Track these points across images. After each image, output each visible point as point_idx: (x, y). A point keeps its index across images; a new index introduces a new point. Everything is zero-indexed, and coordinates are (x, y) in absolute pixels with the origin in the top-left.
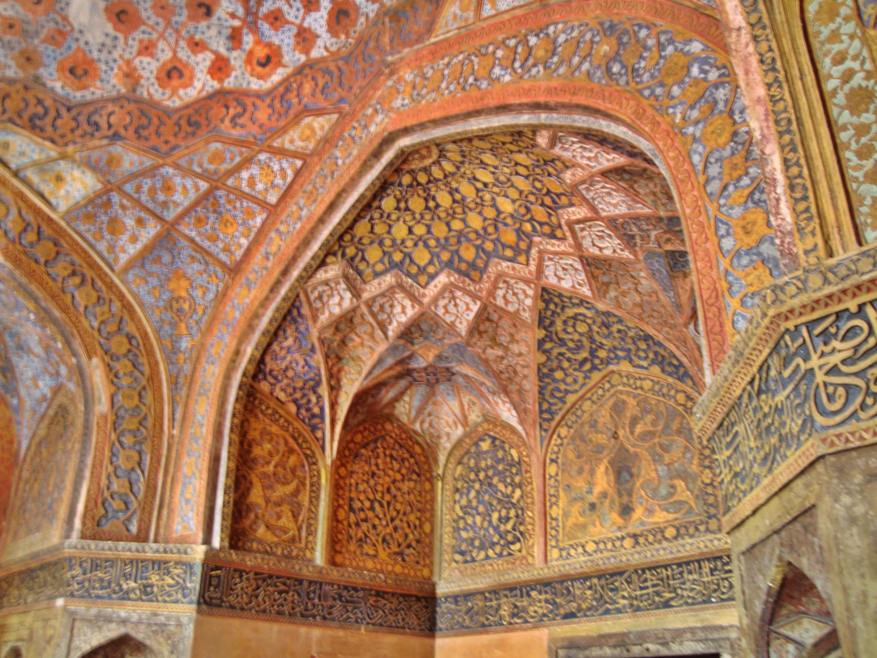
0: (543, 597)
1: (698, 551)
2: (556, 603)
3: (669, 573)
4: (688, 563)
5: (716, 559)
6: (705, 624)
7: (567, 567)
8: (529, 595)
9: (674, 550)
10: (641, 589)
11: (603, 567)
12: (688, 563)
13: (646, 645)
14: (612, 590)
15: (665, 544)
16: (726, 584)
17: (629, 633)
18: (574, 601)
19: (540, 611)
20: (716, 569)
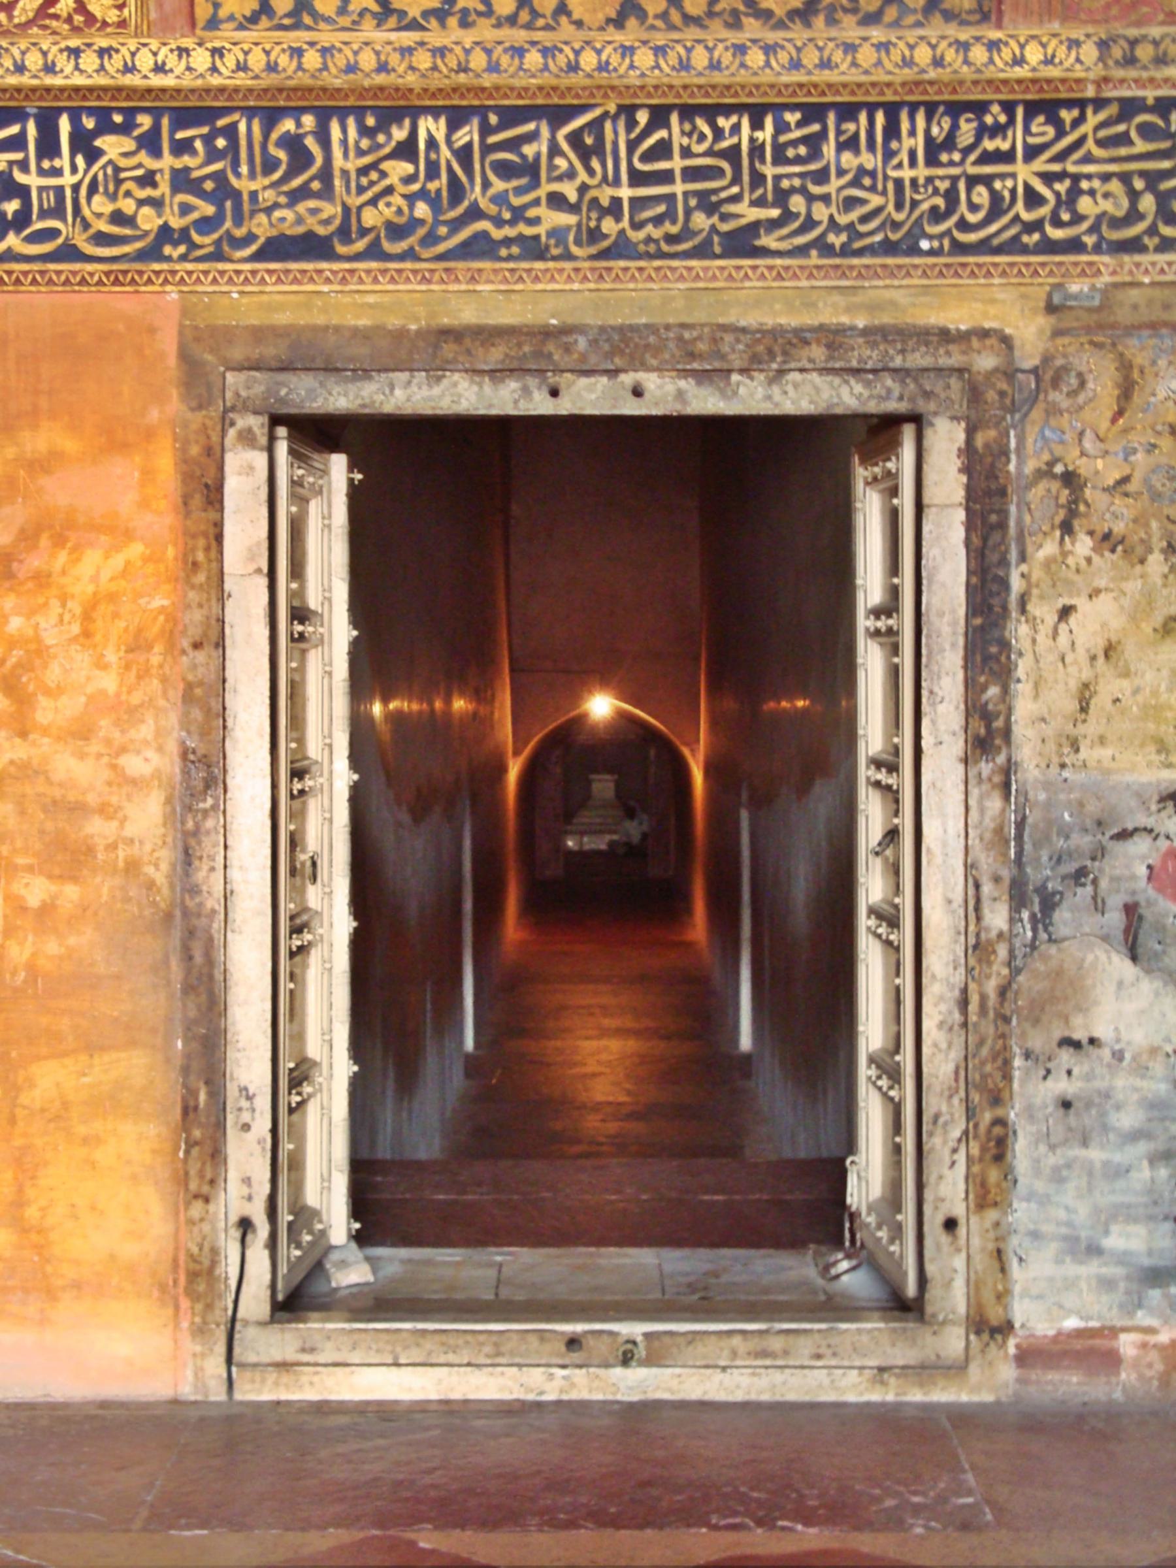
0: (168, 161)
1: (908, 74)
2: (236, 195)
3: (766, 135)
4: (848, 112)
5: (955, 109)
6: (886, 319)
7: (312, 59)
8: (84, 144)
9: (811, 58)
10: (637, 179)
11: (488, 80)
12: (848, 112)
13: (627, 379)
14: (505, 170)
15: (752, 28)
16: (981, 195)
17: (566, 330)
18: (327, 193)
19: (148, 220)
20: (949, 143)
